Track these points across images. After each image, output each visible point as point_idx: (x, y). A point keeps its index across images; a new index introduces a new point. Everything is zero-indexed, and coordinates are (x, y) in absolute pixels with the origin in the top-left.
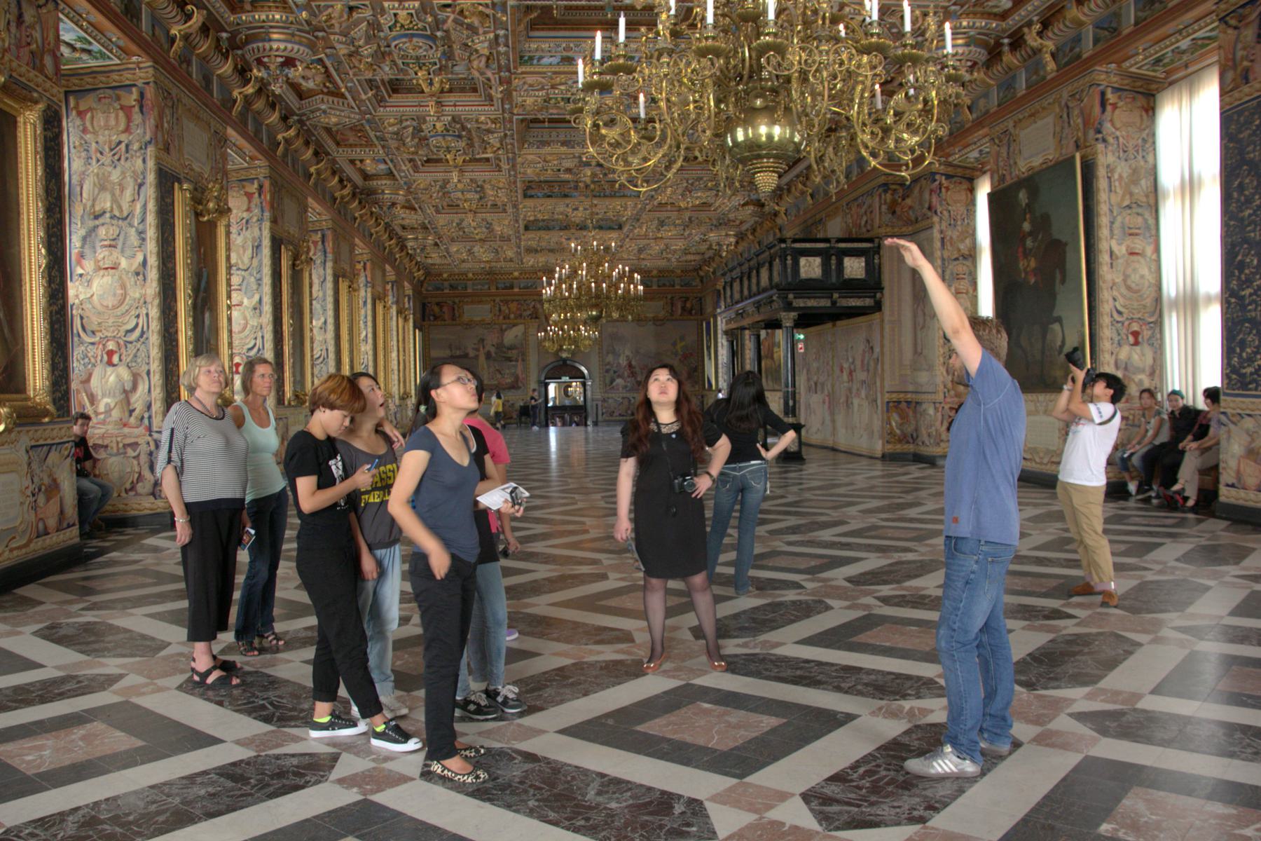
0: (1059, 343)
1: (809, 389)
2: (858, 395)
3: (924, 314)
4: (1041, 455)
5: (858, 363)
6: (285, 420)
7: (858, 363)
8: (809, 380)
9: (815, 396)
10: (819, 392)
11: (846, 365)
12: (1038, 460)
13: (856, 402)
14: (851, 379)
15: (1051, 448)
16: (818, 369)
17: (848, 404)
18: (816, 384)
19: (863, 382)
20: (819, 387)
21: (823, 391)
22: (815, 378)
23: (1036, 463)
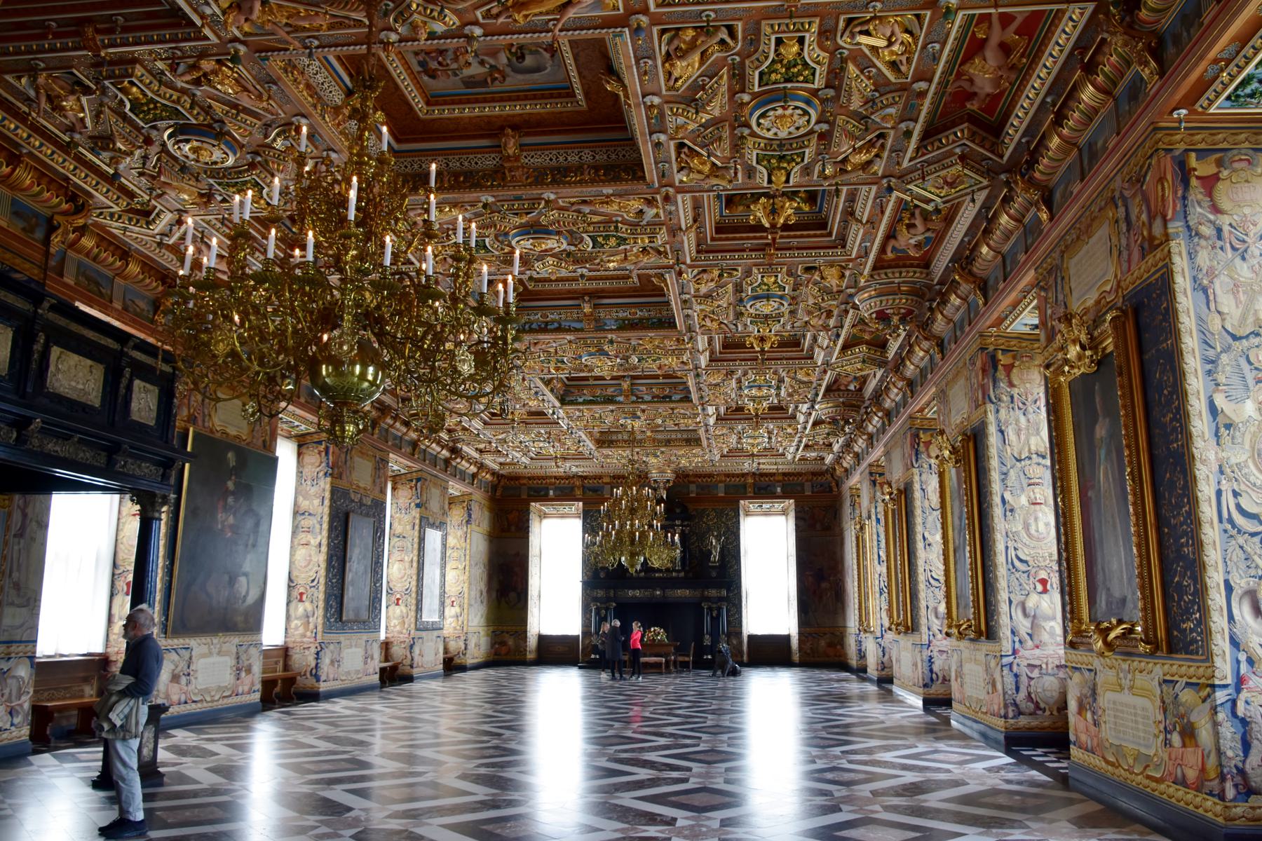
0: (243, 594)
3: (25, 515)
4: (213, 693)
6: (1087, 674)
12: (208, 699)
15: (222, 685)
23: (207, 702)
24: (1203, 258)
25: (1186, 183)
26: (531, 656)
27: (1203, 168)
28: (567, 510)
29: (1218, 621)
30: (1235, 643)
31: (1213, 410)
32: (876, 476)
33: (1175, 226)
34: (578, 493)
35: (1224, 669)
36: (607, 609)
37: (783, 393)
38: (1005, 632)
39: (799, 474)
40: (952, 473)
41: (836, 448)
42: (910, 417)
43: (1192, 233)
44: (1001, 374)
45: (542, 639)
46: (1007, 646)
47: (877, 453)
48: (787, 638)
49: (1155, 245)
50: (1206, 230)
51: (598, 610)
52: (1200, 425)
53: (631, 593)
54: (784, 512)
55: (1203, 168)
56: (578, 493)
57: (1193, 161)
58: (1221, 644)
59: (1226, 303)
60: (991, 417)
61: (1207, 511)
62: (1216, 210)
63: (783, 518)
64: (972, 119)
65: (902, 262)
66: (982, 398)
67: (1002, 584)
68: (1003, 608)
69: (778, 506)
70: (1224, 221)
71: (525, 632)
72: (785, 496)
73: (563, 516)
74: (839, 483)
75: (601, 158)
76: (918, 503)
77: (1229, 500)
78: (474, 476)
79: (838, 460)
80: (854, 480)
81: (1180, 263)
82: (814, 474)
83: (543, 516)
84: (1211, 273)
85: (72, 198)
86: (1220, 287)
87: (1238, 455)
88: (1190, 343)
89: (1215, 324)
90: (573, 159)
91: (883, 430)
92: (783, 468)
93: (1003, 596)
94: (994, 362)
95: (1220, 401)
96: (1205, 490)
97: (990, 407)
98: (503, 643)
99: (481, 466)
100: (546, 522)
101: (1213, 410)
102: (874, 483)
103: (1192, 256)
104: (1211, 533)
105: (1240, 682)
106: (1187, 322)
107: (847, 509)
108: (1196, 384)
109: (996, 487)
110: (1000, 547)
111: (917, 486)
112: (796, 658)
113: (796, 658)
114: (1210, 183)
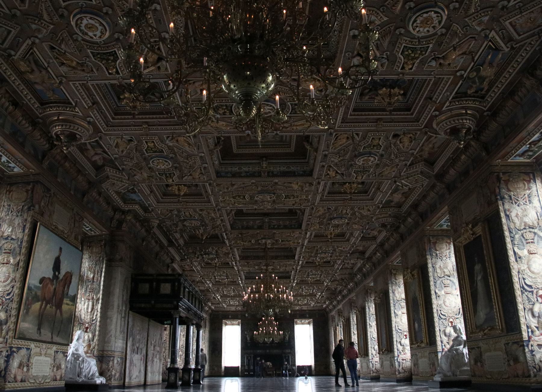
1: (133, 351)
2: (156, 357)
5: (157, 343)
7: (157, 343)
8: (133, 345)
9: (136, 356)
10: (139, 354)
11: (153, 342)
13: (155, 360)
14: (154, 350)
16: (139, 340)
17: (153, 361)
18: (138, 348)
19: (158, 352)
20: (139, 351)
21: (141, 353)
22: (138, 345)
24: (394, 287)
25: (391, 274)
26: (223, 374)
27: (394, 272)
28: (235, 322)
29: (395, 346)
30: (398, 350)
31: (395, 313)
32: (340, 313)
33: (390, 282)
34: (239, 316)
35: (396, 354)
36: (251, 357)
37: (314, 291)
38: (370, 354)
39: (315, 310)
40: (359, 316)
41: (327, 303)
42: (349, 299)
43: (392, 283)
44: (369, 294)
45: (225, 367)
46: (370, 358)
47: (340, 306)
48: (310, 366)
49: (387, 284)
50: (394, 283)
51: (247, 358)
52: (393, 315)
53: (258, 351)
54: (309, 323)
55: (394, 272)
56: (239, 316)
57: (392, 271)
58: (396, 350)
59: (397, 295)
60: (367, 305)
61: (394, 329)
62: (396, 279)
63: (308, 325)
64: (359, 252)
65: (347, 268)
66: (365, 301)
67: (369, 343)
68: (370, 349)
69: (307, 321)
70: (397, 281)
71: (221, 365)
72: (309, 318)
73: (233, 325)
74: (327, 313)
75: (286, 254)
76: (352, 323)
77: (397, 327)
78: (207, 311)
79: (327, 306)
80: (333, 313)
81: (390, 288)
82: (319, 310)
83: (226, 324)
84: (395, 290)
85: (172, 259)
86: (396, 292)
87: (398, 320)
88: (391, 301)
89: (395, 299)
90: (280, 254)
91: (342, 301)
92: (310, 309)
93: (370, 346)
94: (367, 291)
95: (396, 311)
96: (393, 325)
97: (366, 303)
98: (214, 369)
99: (210, 308)
100: (227, 327)
101: (395, 313)
102: (339, 315)
103: (392, 287)
104: (394, 333)
105: (398, 356)
106: (391, 298)
107: (330, 322)
108: (392, 308)
109: (368, 321)
110: (369, 335)
111: (351, 318)
112: (314, 373)
113: (314, 373)
114: (395, 274)
